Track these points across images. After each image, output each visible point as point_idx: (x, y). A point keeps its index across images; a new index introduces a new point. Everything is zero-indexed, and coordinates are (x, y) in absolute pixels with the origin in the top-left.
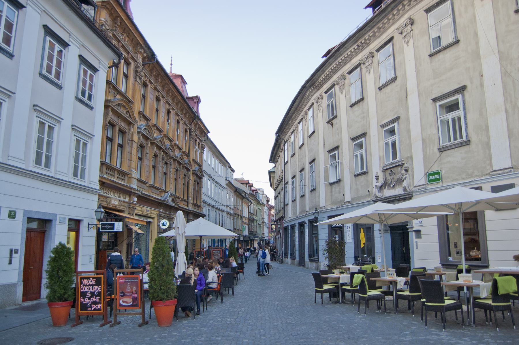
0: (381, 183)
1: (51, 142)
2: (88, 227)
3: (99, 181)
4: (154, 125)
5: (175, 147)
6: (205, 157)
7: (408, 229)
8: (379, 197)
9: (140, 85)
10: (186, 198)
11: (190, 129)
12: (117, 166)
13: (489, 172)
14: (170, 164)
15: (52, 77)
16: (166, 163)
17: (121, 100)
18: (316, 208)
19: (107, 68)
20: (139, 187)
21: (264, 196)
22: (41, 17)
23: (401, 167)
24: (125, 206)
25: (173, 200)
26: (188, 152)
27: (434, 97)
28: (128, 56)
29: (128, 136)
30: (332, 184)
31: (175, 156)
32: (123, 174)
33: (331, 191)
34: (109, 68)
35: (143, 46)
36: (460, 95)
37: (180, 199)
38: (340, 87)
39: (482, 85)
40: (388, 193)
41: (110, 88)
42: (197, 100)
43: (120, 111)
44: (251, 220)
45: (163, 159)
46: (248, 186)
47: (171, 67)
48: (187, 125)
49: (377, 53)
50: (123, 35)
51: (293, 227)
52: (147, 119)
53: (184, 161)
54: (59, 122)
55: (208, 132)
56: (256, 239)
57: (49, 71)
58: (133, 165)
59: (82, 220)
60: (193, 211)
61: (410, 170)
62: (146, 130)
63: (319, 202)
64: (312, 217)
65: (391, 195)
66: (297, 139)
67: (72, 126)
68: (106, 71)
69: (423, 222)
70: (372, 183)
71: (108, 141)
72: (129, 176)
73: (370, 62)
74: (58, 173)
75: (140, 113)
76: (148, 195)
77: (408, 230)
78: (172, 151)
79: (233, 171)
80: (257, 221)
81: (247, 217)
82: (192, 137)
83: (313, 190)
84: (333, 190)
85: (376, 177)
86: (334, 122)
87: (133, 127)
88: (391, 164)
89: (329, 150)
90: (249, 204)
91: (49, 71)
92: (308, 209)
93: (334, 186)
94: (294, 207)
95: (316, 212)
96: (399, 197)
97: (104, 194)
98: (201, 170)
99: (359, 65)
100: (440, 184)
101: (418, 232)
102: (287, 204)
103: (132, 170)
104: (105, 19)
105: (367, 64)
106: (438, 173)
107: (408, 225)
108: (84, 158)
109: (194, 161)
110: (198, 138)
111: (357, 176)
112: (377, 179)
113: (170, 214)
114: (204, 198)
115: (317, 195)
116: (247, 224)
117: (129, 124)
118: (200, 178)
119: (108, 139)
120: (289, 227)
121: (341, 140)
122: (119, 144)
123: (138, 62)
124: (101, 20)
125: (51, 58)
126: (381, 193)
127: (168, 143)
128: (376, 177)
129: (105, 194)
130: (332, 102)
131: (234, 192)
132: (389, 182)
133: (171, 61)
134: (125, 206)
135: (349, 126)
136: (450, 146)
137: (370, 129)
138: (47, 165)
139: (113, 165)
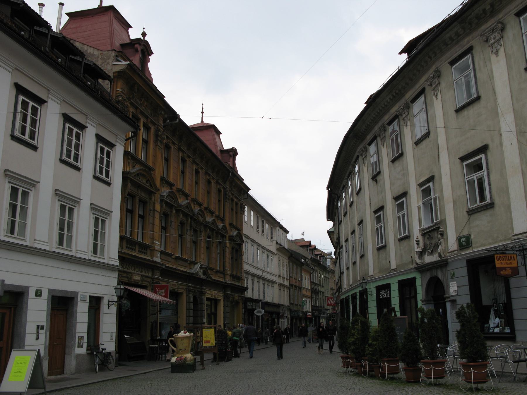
0: (420, 249)
1: (71, 223)
2: (109, 304)
3: (119, 256)
4: (179, 190)
5: (205, 212)
6: (246, 218)
7: (445, 298)
8: (419, 264)
9: (161, 148)
10: (222, 270)
11: (224, 188)
12: (138, 239)
13: (511, 236)
14: (200, 231)
15: (72, 160)
16: (195, 231)
17: (140, 170)
18: (363, 277)
19: (124, 140)
20: (164, 260)
22: (60, 106)
23: (437, 231)
24: (148, 282)
25: (204, 273)
26: (222, 216)
27: (461, 155)
28: (147, 121)
31: (206, 222)
32: (144, 248)
33: (379, 258)
34: (126, 140)
35: (163, 107)
36: (483, 155)
37: (214, 271)
38: (381, 140)
39: (501, 144)
41: (128, 158)
42: (233, 153)
43: (139, 181)
44: (315, 292)
45: (191, 227)
46: (310, 249)
47: (202, 116)
48: (220, 184)
49: (412, 104)
50: (141, 100)
52: (171, 185)
53: (217, 227)
54: (78, 203)
55: (249, 189)
56: (322, 315)
57: (69, 156)
58: (157, 235)
59: (104, 297)
60: (230, 283)
61: (445, 234)
62: (169, 197)
63: (368, 270)
66: (348, 196)
67: (91, 204)
68: (123, 144)
70: (414, 249)
71: (128, 214)
72: (151, 248)
74: (78, 252)
75: (162, 179)
76: (174, 269)
77: (446, 300)
78: (202, 217)
79: (287, 232)
80: (323, 293)
81: (309, 288)
82: (227, 197)
83: (362, 256)
85: (416, 241)
86: (379, 178)
87: (154, 196)
89: (375, 210)
90: (312, 272)
91: (69, 156)
94: (348, 275)
95: (364, 281)
96: (436, 264)
97: (124, 270)
98: (240, 235)
102: (343, 273)
103: (155, 242)
104: (121, 89)
105: (404, 116)
107: (445, 295)
108: (103, 234)
109: (231, 225)
110: (236, 197)
111: (401, 240)
112: (418, 244)
113: (202, 289)
114: (246, 267)
116: (309, 298)
117: (150, 193)
118: (240, 246)
119: (128, 211)
121: (384, 199)
122: (140, 216)
123: (158, 125)
124: (118, 90)
125: (69, 144)
126: (421, 259)
127: (196, 209)
128: (416, 241)
129: (126, 270)
131: (289, 258)
132: (428, 248)
133: (203, 108)
134: (148, 282)
135: (392, 184)
136: (477, 209)
137: (409, 187)
138: (69, 244)
139: (134, 239)
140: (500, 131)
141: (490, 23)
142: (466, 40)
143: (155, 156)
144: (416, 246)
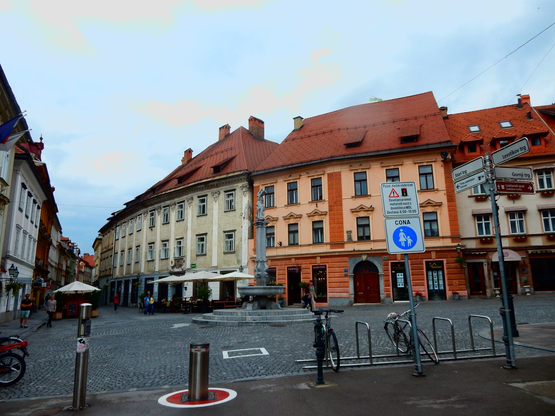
21: (78, 250)
30: (149, 261)
33: (148, 265)
38: (158, 212)
39: (212, 234)
40: (176, 270)
51: (120, 283)
63: (141, 270)
64: (136, 278)
65: (177, 271)
69: (188, 284)
73: (174, 207)
83: (137, 263)
84: (149, 264)
86: (153, 228)
88: (178, 257)
92: (132, 273)
93: (150, 262)
99: (168, 206)
100: (195, 269)
101: (186, 288)
105: (173, 207)
106: (195, 265)
115: (139, 266)
120: (116, 283)
130: (153, 218)
135: (161, 234)
140: (212, 229)
141: (215, 190)
142: (205, 191)
144: (170, 263)
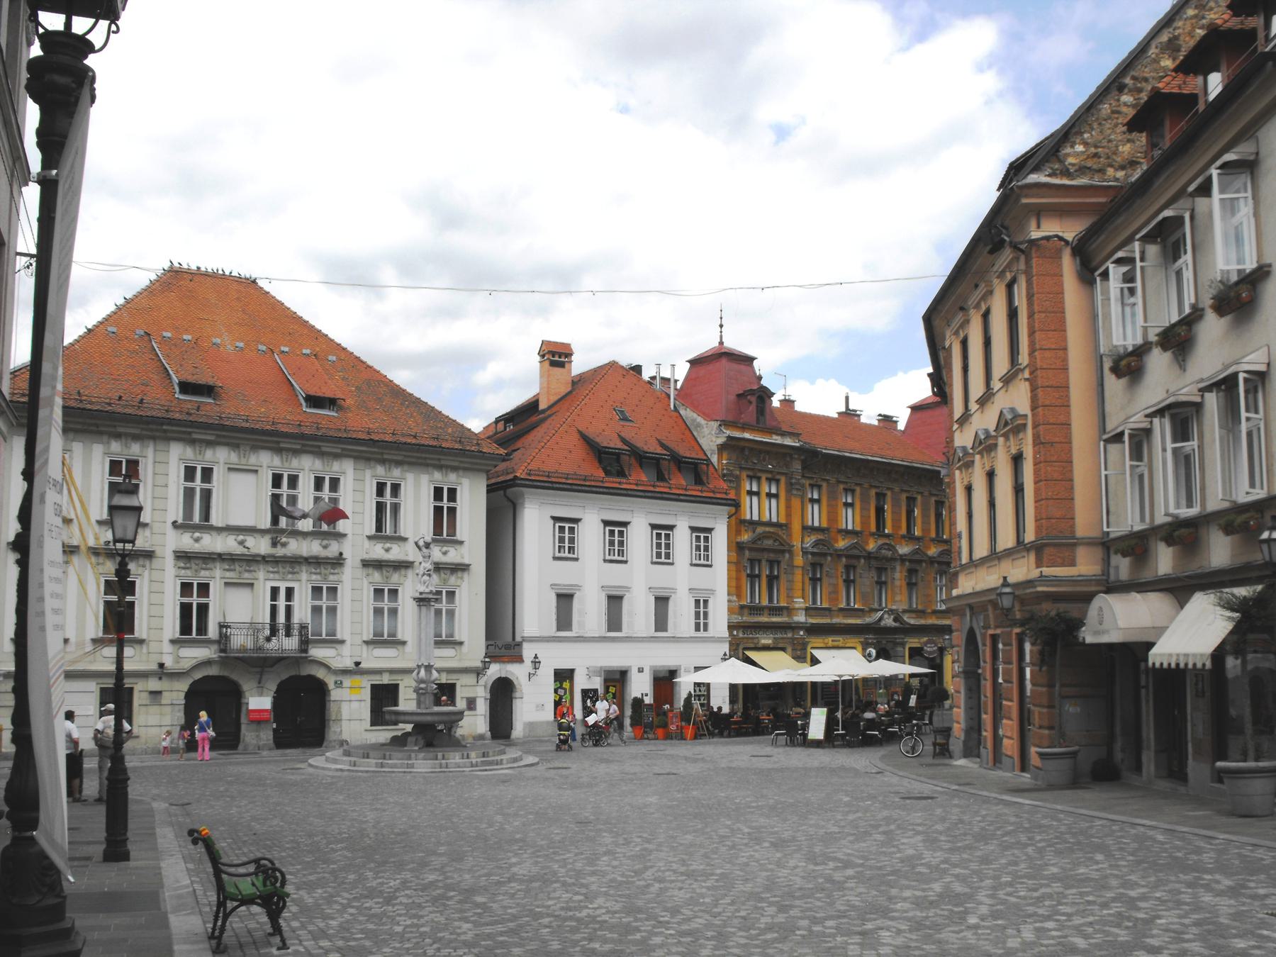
25: (895, 620)
29: (783, 566)
129: (751, 636)
143: (788, 507)
